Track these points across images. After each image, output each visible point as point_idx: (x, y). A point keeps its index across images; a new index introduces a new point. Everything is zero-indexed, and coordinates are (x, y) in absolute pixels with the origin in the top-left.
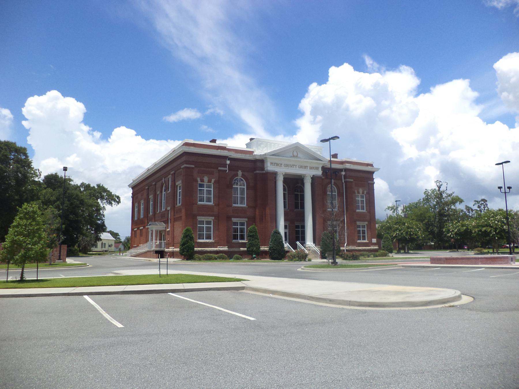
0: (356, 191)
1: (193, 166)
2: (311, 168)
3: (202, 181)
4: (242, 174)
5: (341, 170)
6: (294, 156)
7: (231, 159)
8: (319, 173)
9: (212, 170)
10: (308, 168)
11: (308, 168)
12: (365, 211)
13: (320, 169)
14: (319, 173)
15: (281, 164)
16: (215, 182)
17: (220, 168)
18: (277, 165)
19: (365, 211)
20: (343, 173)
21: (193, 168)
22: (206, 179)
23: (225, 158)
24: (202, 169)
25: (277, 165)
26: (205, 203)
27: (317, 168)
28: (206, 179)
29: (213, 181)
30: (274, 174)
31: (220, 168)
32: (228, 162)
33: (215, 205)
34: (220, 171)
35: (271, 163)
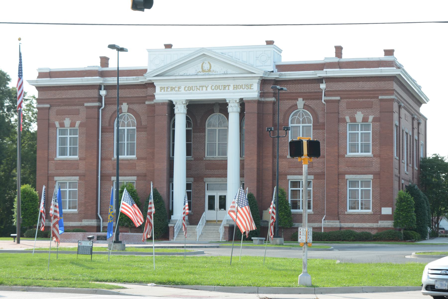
0: (348, 119)
1: (48, 106)
2: (236, 87)
3: (62, 125)
4: (129, 108)
5: (320, 80)
6: (203, 71)
7: (107, 87)
8: (253, 93)
9: (77, 107)
10: (231, 88)
11: (231, 88)
12: (370, 154)
13: (256, 87)
14: (253, 93)
15: (179, 88)
16: (80, 125)
17: (86, 104)
18: (172, 89)
19: (370, 154)
20: (323, 86)
21: (49, 108)
22: (67, 122)
23: (99, 87)
24: (63, 108)
25: (172, 89)
26: (68, 157)
27: (249, 87)
28: (67, 122)
29: (78, 123)
30: (171, 105)
31: (86, 104)
32: (103, 93)
33: (80, 159)
34: (88, 107)
35: (162, 88)
